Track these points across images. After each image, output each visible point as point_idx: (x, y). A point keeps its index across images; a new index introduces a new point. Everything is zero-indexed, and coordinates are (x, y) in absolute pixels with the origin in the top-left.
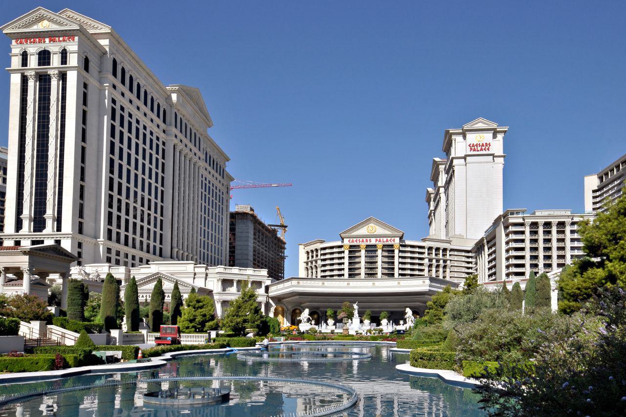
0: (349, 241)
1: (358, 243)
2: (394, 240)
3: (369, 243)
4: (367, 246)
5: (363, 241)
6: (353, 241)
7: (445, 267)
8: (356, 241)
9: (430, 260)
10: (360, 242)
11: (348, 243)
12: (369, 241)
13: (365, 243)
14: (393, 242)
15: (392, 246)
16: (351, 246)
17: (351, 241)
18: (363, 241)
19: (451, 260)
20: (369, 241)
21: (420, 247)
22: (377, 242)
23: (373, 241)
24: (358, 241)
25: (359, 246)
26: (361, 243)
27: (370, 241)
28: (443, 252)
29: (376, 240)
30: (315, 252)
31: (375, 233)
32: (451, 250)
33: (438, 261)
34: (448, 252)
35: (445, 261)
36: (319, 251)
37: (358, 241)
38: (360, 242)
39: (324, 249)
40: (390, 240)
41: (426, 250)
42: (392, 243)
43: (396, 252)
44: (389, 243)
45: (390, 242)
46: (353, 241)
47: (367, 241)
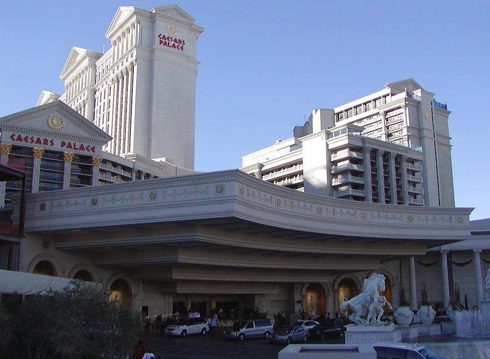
0: (12, 137)
1: (29, 144)
2: (93, 149)
3: (49, 147)
6: (19, 138)
8: (26, 139)
11: (10, 140)
15: (88, 159)
16: (14, 148)
17: (15, 137)
18: (39, 141)
21: (125, 168)
22: (65, 147)
23: (57, 147)
24: (29, 140)
25: (30, 151)
26: (34, 144)
27: (52, 144)
29: (63, 144)
31: (62, 131)
37: (29, 140)
42: (90, 154)
43: (96, 170)
44: (85, 153)
45: (86, 151)
46: (19, 138)
47: (46, 142)
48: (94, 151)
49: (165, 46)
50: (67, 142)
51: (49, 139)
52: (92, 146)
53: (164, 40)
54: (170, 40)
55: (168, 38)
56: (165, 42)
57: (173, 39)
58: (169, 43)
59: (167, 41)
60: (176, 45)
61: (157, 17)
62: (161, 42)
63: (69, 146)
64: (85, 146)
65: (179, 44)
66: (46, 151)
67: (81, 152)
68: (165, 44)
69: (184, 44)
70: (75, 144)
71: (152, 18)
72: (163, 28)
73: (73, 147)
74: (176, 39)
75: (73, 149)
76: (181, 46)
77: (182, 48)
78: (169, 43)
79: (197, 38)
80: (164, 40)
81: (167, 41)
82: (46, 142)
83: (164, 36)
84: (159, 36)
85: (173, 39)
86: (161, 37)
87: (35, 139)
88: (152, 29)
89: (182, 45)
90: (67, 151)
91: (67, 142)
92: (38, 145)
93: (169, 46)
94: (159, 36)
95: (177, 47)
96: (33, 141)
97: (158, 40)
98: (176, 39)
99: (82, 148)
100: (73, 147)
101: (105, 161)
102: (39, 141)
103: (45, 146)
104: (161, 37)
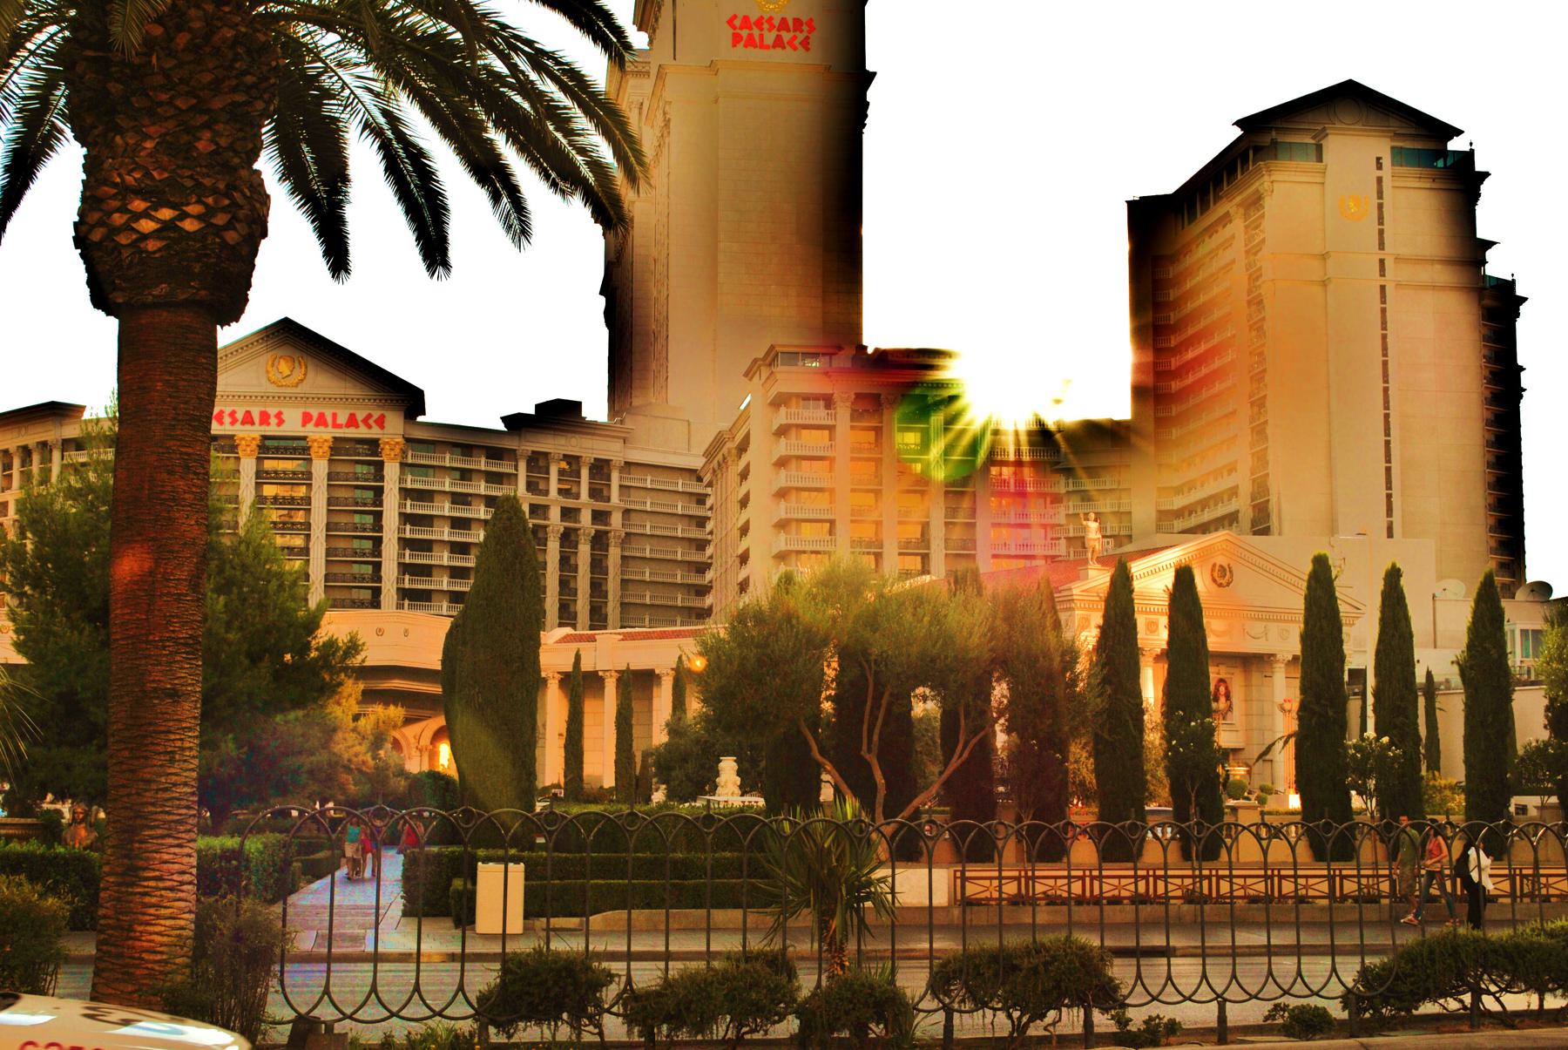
3: (272, 429)
4: (269, 447)
5: (248, 419)
7: (600, 542)
10: (233, 423)
12: (273, 421)
13: (257, 431)
15: (373, 445)
19: (627, 512)
20: (273, 421)
22: (310, 426)
23: (292, 425)
24: (227, 420)
26: (238, 426)
27: (281, 422)
28: (592, 476)
29: (307, 418)
30: (36, 458)
32: (628, 465)
33: (567, 513)
34: (615, 476)
35: (600, 516)
36: (56, 455)
38: (233, 423)
39: (78, 444)
40: (365, 421)
41: (522, 466)
42: (374, 432)
43: (391, 471)
44: (362, 432)
47: (265, 418)
48: (382, 427)
49: (751, 49)
50: (315, 413)
51: (272, 411)
53: (745, 33)
54: (766, 26)
56: (750, 37)
58: (761, 37)
59: (756, 32)
60: (786, 36)
62: (736, 39)
63: (321, 421)
66: (265, 438)
67: (352, 433)
68: (750, 42)
70: (334, 416)
73: (330, 421)
74: (784, 20)
76: (801, 36)
78: (761, 37)
81: (756, 32)
82: (265, 418)
83: (746, 18)
84: (730, 22)
85: (776, 22)
86: (737, 23)
87: (240, 416)
89: (805, 34)
90: (311, 431)
91: (315, 413)
92: (248, 427)
93: (763, 46)
94: (730, 22)
95: (791, 43)
98: (784, 20)
99: (352, 421)
100: (330, 421)
102: (248, 419)
103: (264, 427)
104: (737, 23)
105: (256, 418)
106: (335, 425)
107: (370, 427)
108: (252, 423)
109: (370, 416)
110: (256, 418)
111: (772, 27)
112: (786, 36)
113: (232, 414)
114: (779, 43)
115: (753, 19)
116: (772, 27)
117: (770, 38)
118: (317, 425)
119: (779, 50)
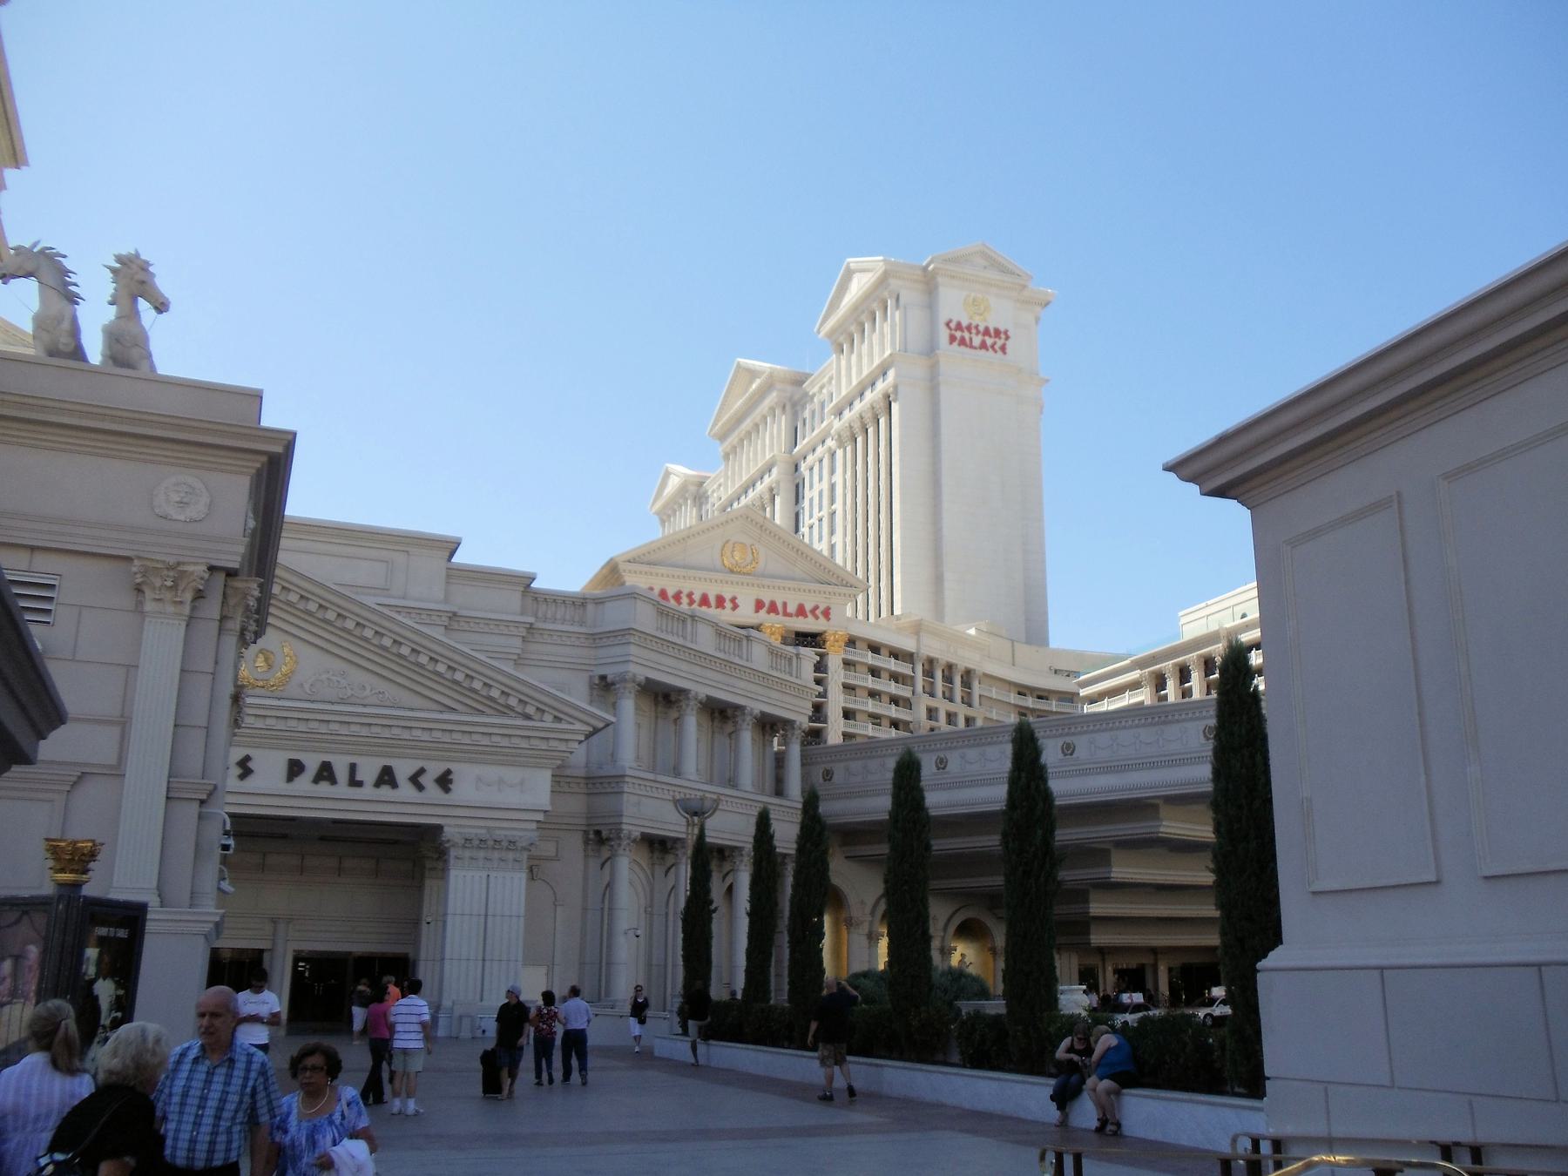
2: (826, 613)
5: (705, 601)
9: (932, 713)
12: (728, 605)
14: (822, 619)
20: (728, 605)
22: (763, 612)
24: (685, 600)
27: (735, 607)
29: (759, 605)
40: (813, 611)
44: (808, 625)
51: (728, 597)
52: (822, 607)
53: (958, 334)
55: (969, 328)
57: (981, 329)
59: (967, 335)
60: (989, 341)
61: (940, 279)
62: (952, 339)
63: (773, 608)
64: (808, 607)
65: (995, 340)
68: (963, 342)
69: (1007, 338)
70: (785, 605)
71: (929, 283)
72: (953, 305)
75: (780, 617)
76: (1000, 343)
77: (1003, 348)
79: (1037, 320)
80: (960, 334)
81: (967, 335)
84: (948, 324)
85: (981, 329)
86: (953, 325)
87: (697, 597)
88: (931, 306)
93: (971, 347)
96: (692, 602)
97: (944, 334)
99: (801, 611)
101: (851, 642)
104: (953, 325)
105: (712, 600)
106: (786, 614)
107: (817, 618)
108: (709, 606)
109: (816, 608)
110: (712, 600)
111: (978, 333)
112: (989, 341)
113: (690, 595)
114: (983, 346)
115: (964, 324)
116: (978, 333)
117: (977, 340)
118: (769, 612)
119: (983, 352)
